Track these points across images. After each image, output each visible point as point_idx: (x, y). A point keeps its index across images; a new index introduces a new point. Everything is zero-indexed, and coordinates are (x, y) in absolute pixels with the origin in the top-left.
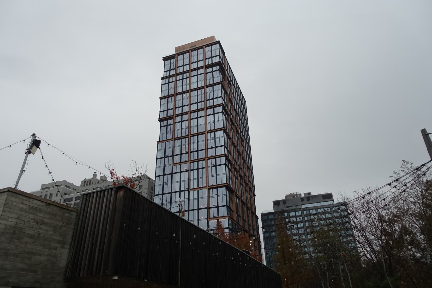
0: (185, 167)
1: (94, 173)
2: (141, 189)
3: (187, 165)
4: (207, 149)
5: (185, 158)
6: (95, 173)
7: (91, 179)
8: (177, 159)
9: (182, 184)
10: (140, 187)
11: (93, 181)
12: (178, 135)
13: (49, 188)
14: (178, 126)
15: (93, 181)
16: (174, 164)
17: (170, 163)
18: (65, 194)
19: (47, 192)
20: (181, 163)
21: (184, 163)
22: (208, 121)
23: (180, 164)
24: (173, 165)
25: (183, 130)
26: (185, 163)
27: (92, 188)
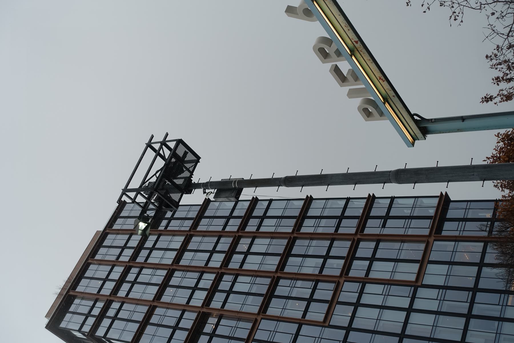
3: (347, 286)
9: (392, 302)
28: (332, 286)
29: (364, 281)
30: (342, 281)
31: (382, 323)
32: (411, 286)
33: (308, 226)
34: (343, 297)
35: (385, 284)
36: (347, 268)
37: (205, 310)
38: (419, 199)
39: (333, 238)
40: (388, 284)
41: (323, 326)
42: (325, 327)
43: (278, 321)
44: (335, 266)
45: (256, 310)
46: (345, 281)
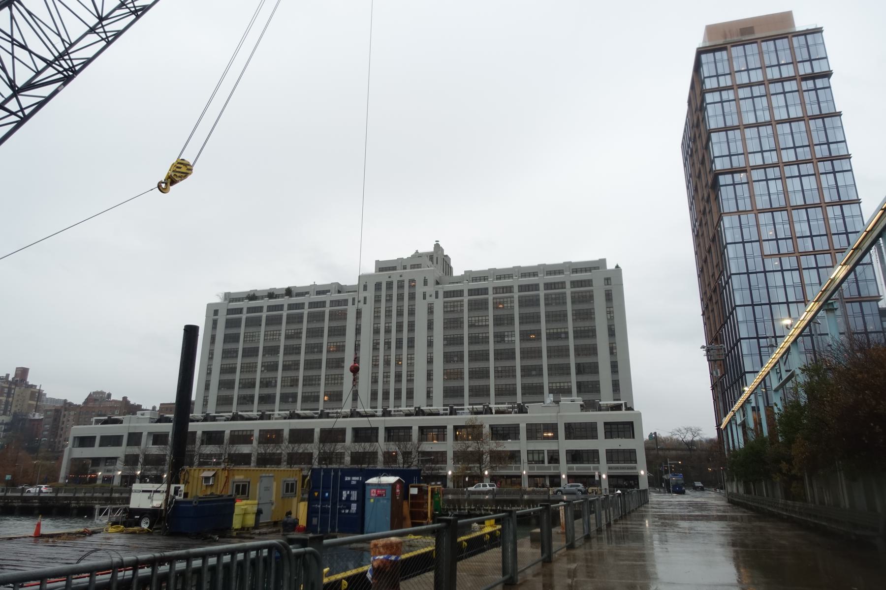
0: (787, 263)
1: (435, 243)
2: (608, 285)
4: (828, 235)
5: (786, 246)
6: (436, 241)
7: (432, 252)
8: (770, 248)
9: (790, 291)
10: (606, 281)
11: (437, 258)
12: (762, 203)
13: (394, 268)
14: (759, 188)
15: (437, 258)
16: (764, 256)
17: (757, 253)
18: (438, 283)
19: (401, 276)
20: (779, 255)
21: (788, 255)
22: (824, 185)
23: (779, 256)
24: (764, 257)
25: (772, 197)
26: (790, 255)
27: (494, 275)
28: (791, 249)
29: (799, 269)
30: (796, 254)
31: (775, 289)
32: (804, 298)
33: (833, 212)
34: (785, 260)
35: (801, 282)
36: (806, 254)
37: (748, 169)
38: (875, 282)
39: (828, 235)
40: (802, 284)
41: (762, 255)
42: (762, 257)
43: (757, 225)
44: (806, 245)
45: (759, 207)
46: (797, 257)
